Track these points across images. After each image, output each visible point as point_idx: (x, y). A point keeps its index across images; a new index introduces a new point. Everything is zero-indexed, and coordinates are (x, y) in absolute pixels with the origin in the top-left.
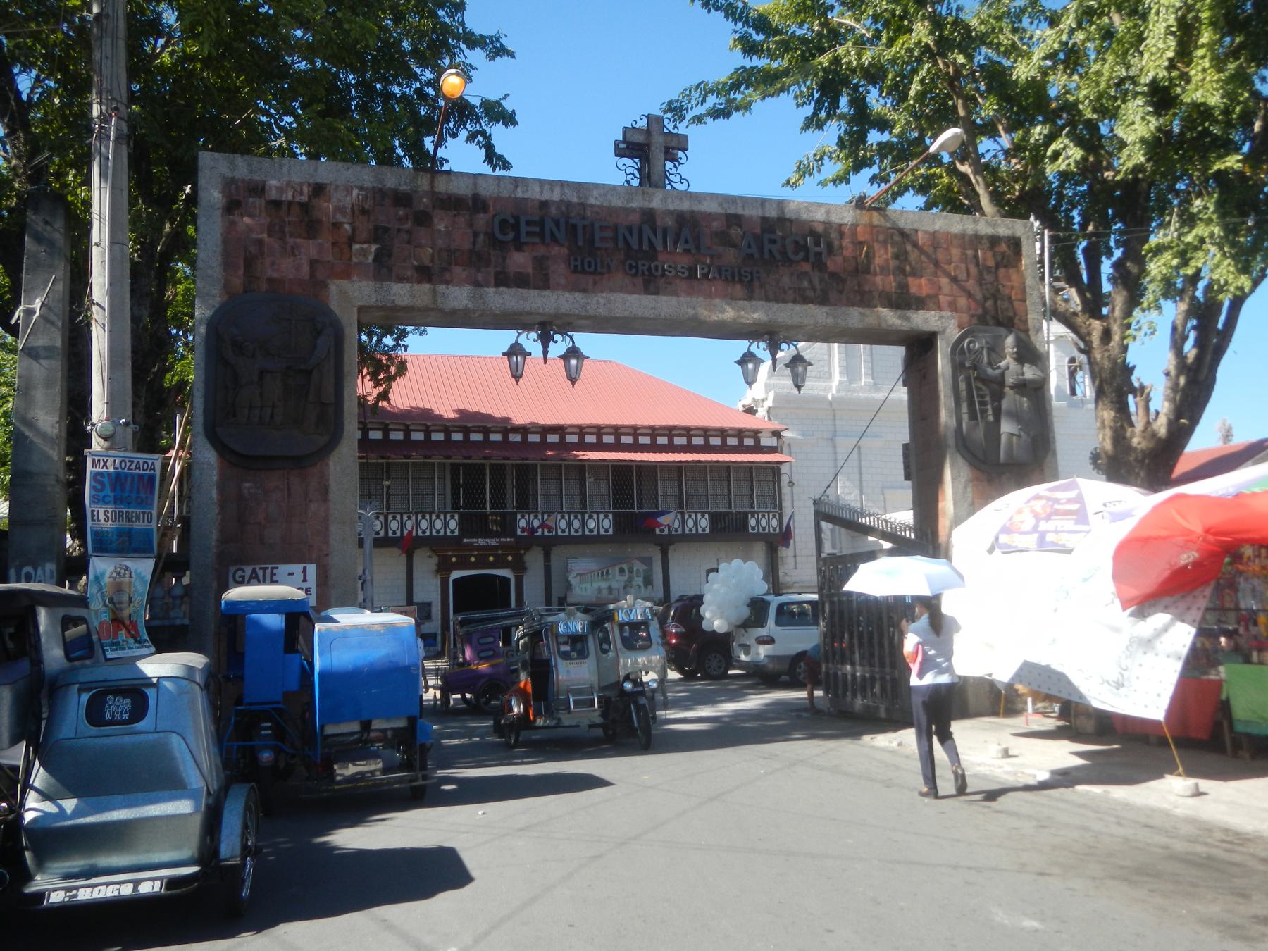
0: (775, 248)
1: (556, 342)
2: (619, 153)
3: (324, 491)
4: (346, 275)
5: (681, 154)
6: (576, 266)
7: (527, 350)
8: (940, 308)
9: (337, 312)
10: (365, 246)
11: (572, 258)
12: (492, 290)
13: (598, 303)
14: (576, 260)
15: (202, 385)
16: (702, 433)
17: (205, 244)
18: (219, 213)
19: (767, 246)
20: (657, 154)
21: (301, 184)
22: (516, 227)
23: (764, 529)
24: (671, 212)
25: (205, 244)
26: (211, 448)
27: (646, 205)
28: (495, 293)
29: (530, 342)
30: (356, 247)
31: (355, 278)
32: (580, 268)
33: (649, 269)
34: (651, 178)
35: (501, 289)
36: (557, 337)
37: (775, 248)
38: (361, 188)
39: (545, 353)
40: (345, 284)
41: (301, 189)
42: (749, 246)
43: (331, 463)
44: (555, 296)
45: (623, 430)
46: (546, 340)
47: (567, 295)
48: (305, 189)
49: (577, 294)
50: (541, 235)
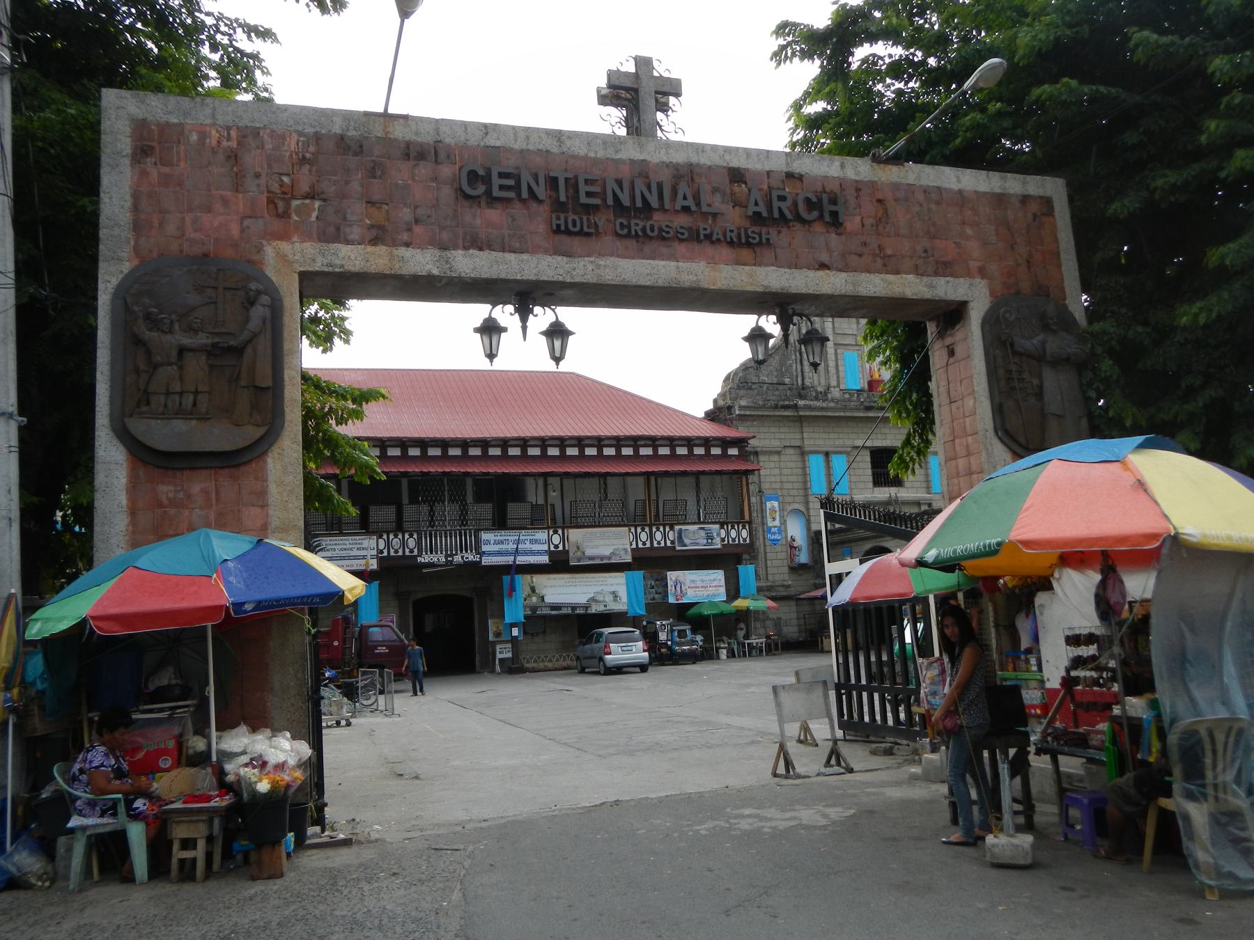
0: (784, 205)
1: (536, 316)
2: (604, 100)
3: (262, 494)
4: (284, 236)
5: (672, 100)
6: (558, 226)
7: (503, 325)
8: (969, 274)
9: (274, 279)
10: (307, 201)
11: (554, 216)
12: (460, 252)
13: (583, 269)
14: (558, 218)
15: (107, 367)
16: (668, 443)
17: (110, 198)
18: (127, 161)
19: (776, 204)
20: (648, 101)
21: (229, 129)
22: (487, 179)
23: (734, 540)
24: (668, 165)
25: (110, 198)
26: (119, 444)
27: (638, 156)
28: (464, 256)
29: (505, 315)
30: (295, 203)
31: (295, 239)
32: (563, 228)
33: (644, 230)
34: (638, 125)
35: (471, 251)
36: (537, 309)
37: (784, 205)
38: (300, 134)
39: (524, 328)
40: (285, 246)
41: (229, 134)
42: (756, 204)
43: (269, 460)
44: (535, 260)
45: (587, 442)
46: (524, 312)
47: (549, 258)
48: (233, 133)
49: (560, 258)
50: (517, 188)
